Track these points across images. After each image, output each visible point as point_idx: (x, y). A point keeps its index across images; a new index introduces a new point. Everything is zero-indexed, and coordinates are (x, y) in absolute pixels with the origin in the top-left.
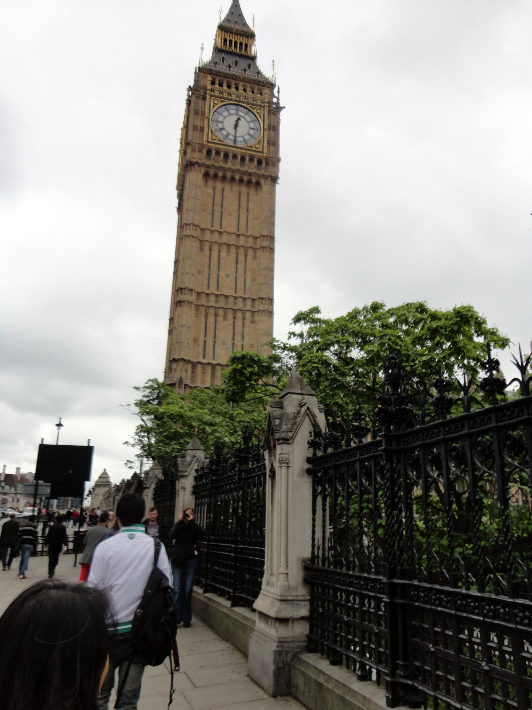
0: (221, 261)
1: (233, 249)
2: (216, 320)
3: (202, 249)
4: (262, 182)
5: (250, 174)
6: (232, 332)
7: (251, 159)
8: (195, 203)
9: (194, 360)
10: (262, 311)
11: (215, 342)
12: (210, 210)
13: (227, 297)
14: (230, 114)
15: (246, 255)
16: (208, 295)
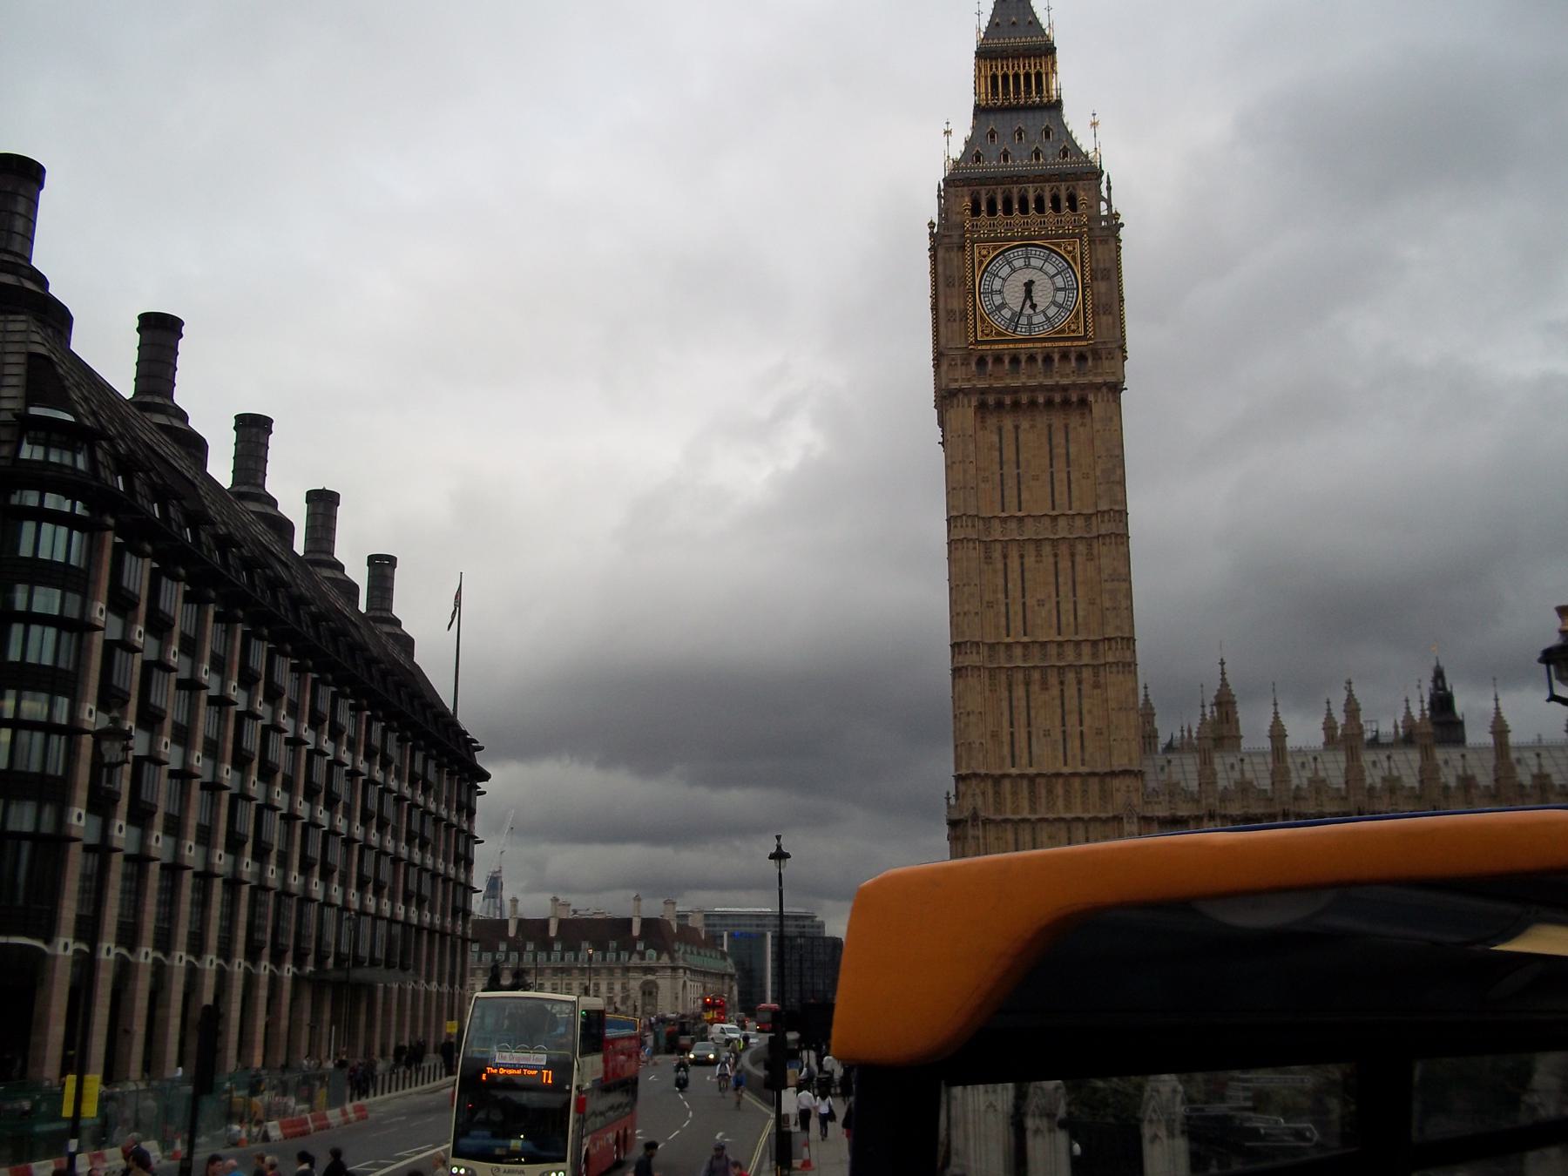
0: (1027, 575)
1: (1047, 549)
2: (1027, 691)
3: (988, 558)
4: (1091, 398)
5: (1065, 388)
6: (1059, 710)
7: (1065, 356)
8: (965, 471)
9: (999, 772)
10: (1111, 664)
11: (1029, 733)
12: (997, 478)
13: (1043, 644)
14: (1014, 270)
15: (1073, 555)
16: (1009, 646)
